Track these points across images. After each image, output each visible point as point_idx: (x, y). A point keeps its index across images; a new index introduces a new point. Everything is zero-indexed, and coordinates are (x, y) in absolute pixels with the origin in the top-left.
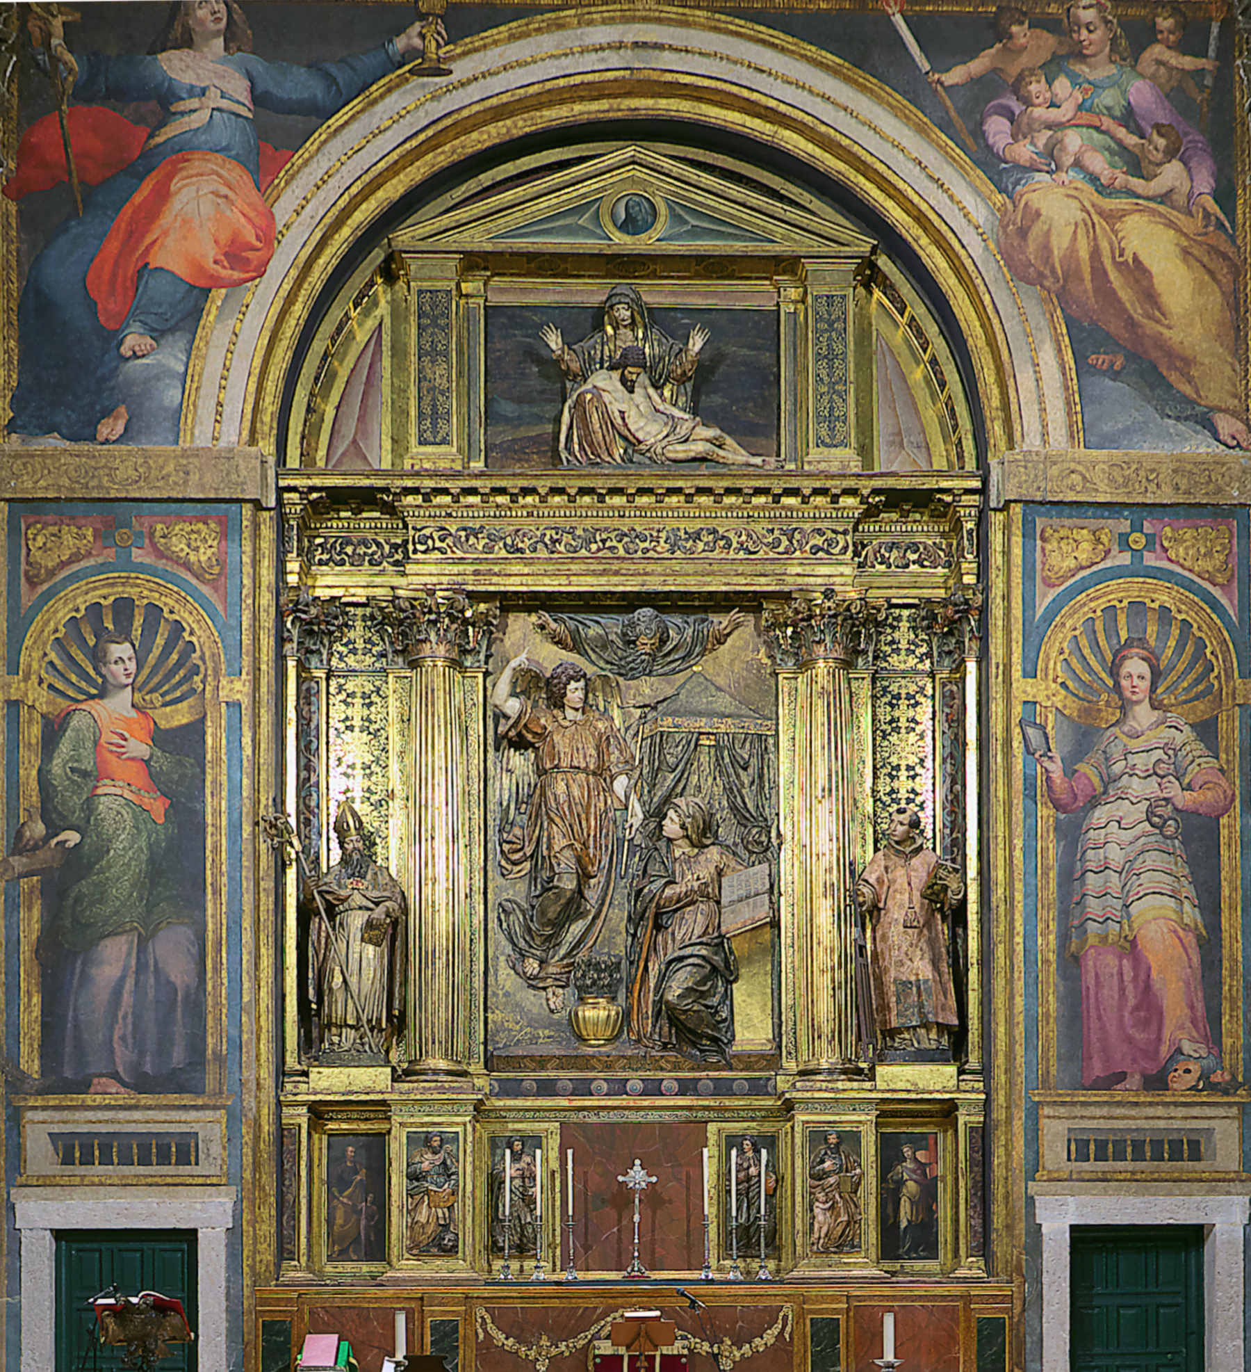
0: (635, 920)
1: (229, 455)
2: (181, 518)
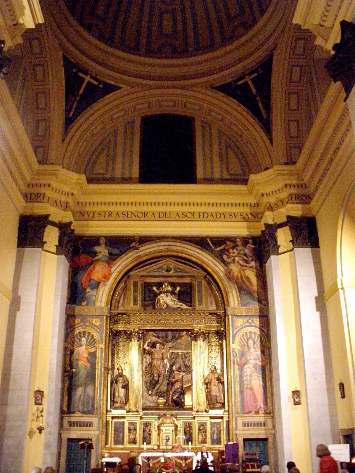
0: (168, 384)
1: (102, 308)
2: (94, 318)
